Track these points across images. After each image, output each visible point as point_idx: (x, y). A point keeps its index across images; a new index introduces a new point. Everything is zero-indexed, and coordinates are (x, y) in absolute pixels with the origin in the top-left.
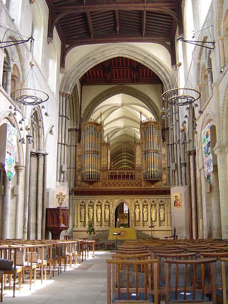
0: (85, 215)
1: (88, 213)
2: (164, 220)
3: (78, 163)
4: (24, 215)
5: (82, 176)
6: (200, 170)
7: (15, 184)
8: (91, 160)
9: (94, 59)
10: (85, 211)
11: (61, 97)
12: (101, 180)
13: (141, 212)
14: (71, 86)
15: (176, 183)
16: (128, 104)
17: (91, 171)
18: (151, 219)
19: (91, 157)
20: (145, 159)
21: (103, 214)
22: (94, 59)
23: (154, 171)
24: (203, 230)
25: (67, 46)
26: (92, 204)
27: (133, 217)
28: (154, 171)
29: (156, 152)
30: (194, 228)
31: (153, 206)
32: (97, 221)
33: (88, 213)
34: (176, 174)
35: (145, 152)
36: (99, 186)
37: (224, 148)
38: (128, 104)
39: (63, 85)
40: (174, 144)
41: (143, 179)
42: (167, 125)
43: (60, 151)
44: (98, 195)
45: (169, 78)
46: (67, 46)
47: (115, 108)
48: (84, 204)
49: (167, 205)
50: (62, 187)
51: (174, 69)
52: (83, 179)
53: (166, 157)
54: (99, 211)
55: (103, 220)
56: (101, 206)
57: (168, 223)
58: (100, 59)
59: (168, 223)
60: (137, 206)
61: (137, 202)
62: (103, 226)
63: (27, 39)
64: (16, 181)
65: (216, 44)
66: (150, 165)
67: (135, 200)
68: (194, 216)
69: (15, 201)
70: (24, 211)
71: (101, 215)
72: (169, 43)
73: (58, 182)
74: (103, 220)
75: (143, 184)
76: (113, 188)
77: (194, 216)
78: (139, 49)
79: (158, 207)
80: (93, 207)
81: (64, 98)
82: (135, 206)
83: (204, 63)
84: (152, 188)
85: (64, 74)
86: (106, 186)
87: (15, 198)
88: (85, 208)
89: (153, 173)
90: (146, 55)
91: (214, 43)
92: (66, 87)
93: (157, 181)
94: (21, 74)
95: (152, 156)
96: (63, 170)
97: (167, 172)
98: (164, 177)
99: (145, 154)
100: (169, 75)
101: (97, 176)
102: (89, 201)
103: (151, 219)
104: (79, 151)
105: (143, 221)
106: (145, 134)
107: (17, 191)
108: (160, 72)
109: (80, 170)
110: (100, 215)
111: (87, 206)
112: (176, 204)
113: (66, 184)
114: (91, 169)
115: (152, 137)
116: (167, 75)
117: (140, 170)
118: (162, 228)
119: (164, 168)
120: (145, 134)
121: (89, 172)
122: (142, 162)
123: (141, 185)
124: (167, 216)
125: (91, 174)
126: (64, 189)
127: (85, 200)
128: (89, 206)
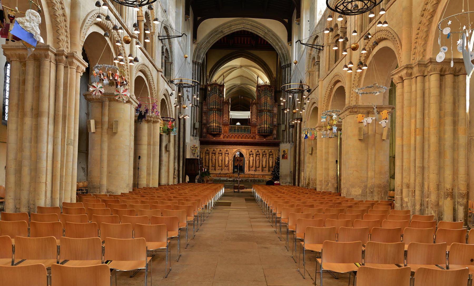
0: (209, 161)
1: (212, 160)
3: (204, 118)
4: (174, 166)
5: (208, 129)
7: (167, 142)
8: (214, 116)
10: (209, 158)
11: (194, 65)
12: (223, 133)
13: (255, 160)
14: (203, 55)
15: (285, 140)
16: (246, 66)
17: (214, 125)
18: (262, 165)
19: (215, 114)
20: (260, 117)
21: (223, 161)
22: (222, 32)
23: (266, 127)
25: (199, 18)
27: (248, 164)
28: (266, 127)
29: (269, 111)
30: (297, 177)
31: (264, 155)
33: (212, 160)
34: (285, 133)
35: (260, 110)
36: (221, 138)
37: (323, 127)
38: (246, 66)
39: (196, 54)
41: (257, 133)
43: (193, 111)
44: (220, 145)
46: (199, 18)
48: (208, 152)
50: (195, 141)
51: (290, 45)
52: (207, 131)
54: (220, 158)
55: (223, 166)
56: (222, 154)
58: (227, 32)
60: (251, 155)
61: (251, 151)
62: (223, 170)
63: (181, 35)
64: (168, 140)
65: (325, 48)
67: (250, 150)
68: (297, 168)
69: (168, 155)
70: (174, 163)
71: (222, 161)
72: (287, 20)
73: (192, 137)
74: (223, 166)
75: (257, 137)
76: (232, 140)
77: (297, 168)
78: (261, 25)
79: (268, 157)
80: (215, 154)
81: (197, 66)
82: (250, 155)
83: (314, 55)
84: (264, 141)
85: (197, 45)
86: (227, 138)
87: (168, 153)
88: (209, 155)
89: (265, 129)
90: (266, 31)
91: (323, 47)
92: (198, 57)
94: (170, 55)
95: (266, 115)
96: (196, 127)
98: (275, 132)
103: (262, 165)
104: (205, 108)
105: (256, 167)
107: (169, 148)
108: (277, 47)
109: (205, 124)
111: (210, 153)
112: (284, 157)
113: (198, 138)
114: (214, 124)
119: (275, 126)
122: (257, 119)
123: (255, 138)
125: (214, 128)
126: (196, 142)
127: (209, 149)
128: (212, 153)
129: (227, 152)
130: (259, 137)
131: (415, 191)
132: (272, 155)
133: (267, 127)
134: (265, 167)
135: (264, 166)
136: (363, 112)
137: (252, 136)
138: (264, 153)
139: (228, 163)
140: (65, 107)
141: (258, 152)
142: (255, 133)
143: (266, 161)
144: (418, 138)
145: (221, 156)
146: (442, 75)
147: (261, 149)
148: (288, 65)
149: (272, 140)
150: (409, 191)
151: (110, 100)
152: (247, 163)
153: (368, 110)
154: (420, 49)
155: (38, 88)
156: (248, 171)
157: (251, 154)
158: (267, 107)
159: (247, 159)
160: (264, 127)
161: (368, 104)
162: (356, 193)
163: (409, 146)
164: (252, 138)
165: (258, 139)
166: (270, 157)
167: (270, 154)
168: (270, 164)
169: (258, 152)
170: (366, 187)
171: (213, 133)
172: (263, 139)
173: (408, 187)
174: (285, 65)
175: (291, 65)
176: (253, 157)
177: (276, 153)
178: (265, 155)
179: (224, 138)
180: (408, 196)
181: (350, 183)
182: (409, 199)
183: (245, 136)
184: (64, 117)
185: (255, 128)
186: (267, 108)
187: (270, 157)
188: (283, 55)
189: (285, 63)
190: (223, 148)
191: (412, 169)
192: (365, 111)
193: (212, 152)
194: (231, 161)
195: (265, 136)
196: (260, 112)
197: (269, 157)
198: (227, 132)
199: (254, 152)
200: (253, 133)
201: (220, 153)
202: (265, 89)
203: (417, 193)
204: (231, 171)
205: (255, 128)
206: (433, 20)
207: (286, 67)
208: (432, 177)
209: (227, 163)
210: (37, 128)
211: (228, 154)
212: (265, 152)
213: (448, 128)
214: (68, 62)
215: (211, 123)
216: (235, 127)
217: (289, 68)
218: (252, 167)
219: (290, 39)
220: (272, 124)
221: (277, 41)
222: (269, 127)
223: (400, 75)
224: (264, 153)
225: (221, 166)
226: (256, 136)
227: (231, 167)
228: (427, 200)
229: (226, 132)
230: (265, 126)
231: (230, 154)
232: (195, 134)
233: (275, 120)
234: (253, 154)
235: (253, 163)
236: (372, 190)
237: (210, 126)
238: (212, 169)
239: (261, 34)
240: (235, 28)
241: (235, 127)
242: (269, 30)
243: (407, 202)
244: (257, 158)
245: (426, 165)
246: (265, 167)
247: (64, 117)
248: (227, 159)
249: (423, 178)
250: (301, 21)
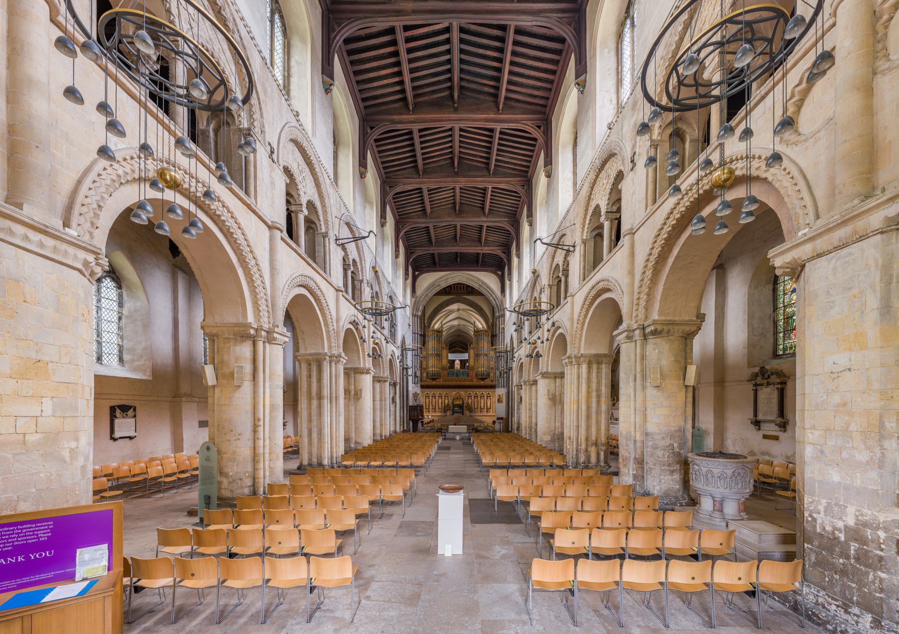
9: (439, 285)
22: (439, 285)
25: (417, 273)
29: (486, 355)
38: (463, 310)
47: (451, 312)
58: (444, 285)
72: (500, 273)
92: (417, 310)
117: (473, 368)
140: (336, 391)
146: (590, 364)
151: (355, 373)
154: (577, 345)
155: (320, 380)
184: (336, 397)
196: (477, 356)
210: (320, 406)
219: (503, 291)
239: (476, 286)
240: (451, 282)
242: (484, 283)
247: (336, 397)
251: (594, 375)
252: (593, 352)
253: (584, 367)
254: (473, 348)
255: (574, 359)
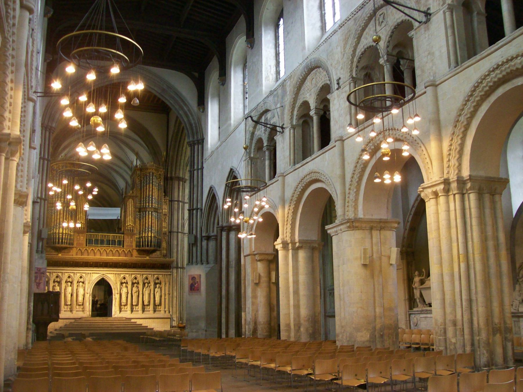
2: (160, 304)
6: (245, 256)
12: (75, 245)
13: (130, 292)
18: (143, 302)
20: (140, 220)
21: (75, 295)
23: (151, 237)
24: (245, 324)
26: (58, 280)
28: (151, 237)
29: (156, 210)
30: (224, 320)
31: (146, 285)
32: (66, 305)
34: (194, 249)
36: (74, 255)
40: (193, 210)
42: (171, 173)
45: (193, 122)
49: (165, 284)
51: (201, 110)
53: (167, 218)
54: (69, 289)
55: (75, 303)
57: (165, 308)
59: (165, 308)
60: (124, 285)
61: (124, 278)
62: (74, 312)
66: (147, 228)
67: (122, 275)
72: (196, 75)
74: (75, 303)
75: (135, 253)
79: (152, 287)
82: (122, 283)
93: (154, 251)
96: (43, 237)
97: (167, 238)
98: (164, 245)
99: (140, 212)
100: (193, 119)
101: (70, 239)
102: (55, 275)
103: (143, 302)
105: (132, 305)
106: (141, 183)
110: (70, 295)
115: (151, 189)
116: (191, 118)
118: (156, 315)
119: (165, 234)
120: (141, 183)
121: (59, 233)
122: (135, 223)
123: (132, 256)
124: (165, 299)
125: (61, 237)
128: (54, 282)
129: (82, 280)
130: (139, 254)
131: (463, 329)
132: (160, 283)
133: (153, 236)
134: (147, 305)
135: (146, 303)
136: (365, 227)
137: (126, 252)
138: (146, 281)
139: (84, 299)
141: (136, 278)
142: (132, 246)
143: (150, 294)
144: (463, 265)
145: (71, 286)
147: (140, 275)
148: (198, 141)
149: (160, 258)
150: (456, 330)
152: (116, 299)
153: (371, 225)
156: (118, 312)
157: (124, 283)
158: (152, 203)
159: (117, 292)
160: (148, 237)
161: (370, 217)
162: (363, 339)
163: (452, 275)
164: (126, 255)
165: (136, 257)
166: (156, 287)
167: (157, 281)
168: (156, 299)
169: (136, 278)
170: (374, 328)
171: (57, 245)
172: (146, 257)
173: (455, 324)
174: (194, 141)
175: (203, 142)
176: (127, 287)
177: (167, 280)
178: (148, 284)
179: (77, 254)
180: (455, 335)
181: (354, 326)
182: (456, 339)
183: (114, 252)
185: (131, 238)
186: (152, 205)
187: (156, 287)
188: (191, 125)
189: (193, 137)
190: (75, 272)
191: (458, 302)
192: (368, 226)
193: (54, 280)
194: (88, 295)
195: (148, 252)
196: (141, 210)
197: (155, 287)
198: (82, 244)
199: (129, 279)
200: (127, 246)
201: (69, 282)
202: (149, 173)
203: (466, 331)
204: (88, 313)
205: (131, 238)
206: (467, 133)
207: (194, 144)
208: (480, 309)
209: (80, 298)
211: (83, 283)
212: (147, 278)
213: (492, 254)
214: (10, 152)
215: (54, 227)
216: (96, 236)
217: (200, 146)
218: (125, 306)
219: (202, 103)
220: (159, 231)
221: (182, 104)
222: (156, 237)
223: (434, 189)
224: (146, 281)
225: (70, 305)
226: (133, 251)
227: (88, 306)
228: (478, 338)
229: (79, 244)
230: (150, 235)
231: (87, 282)
232: (40, 249)
233: (164, 224)
234: (127, 283)
235: (127, 297)
236: (382, 333)
237: (53, 233)
238: (66, 310)
241: (96, 236)
242: (171, 87)
243: (455, 343)
244: (135, 289)
245: (474, 298)
246: (147, 305)
248: (81, 291)
249: (471, 313)
250: (227, 81)
251: (488, 211)
252: (482, 173)
253: (472, 198)
254: (133, 197)
255: (454, 185)
